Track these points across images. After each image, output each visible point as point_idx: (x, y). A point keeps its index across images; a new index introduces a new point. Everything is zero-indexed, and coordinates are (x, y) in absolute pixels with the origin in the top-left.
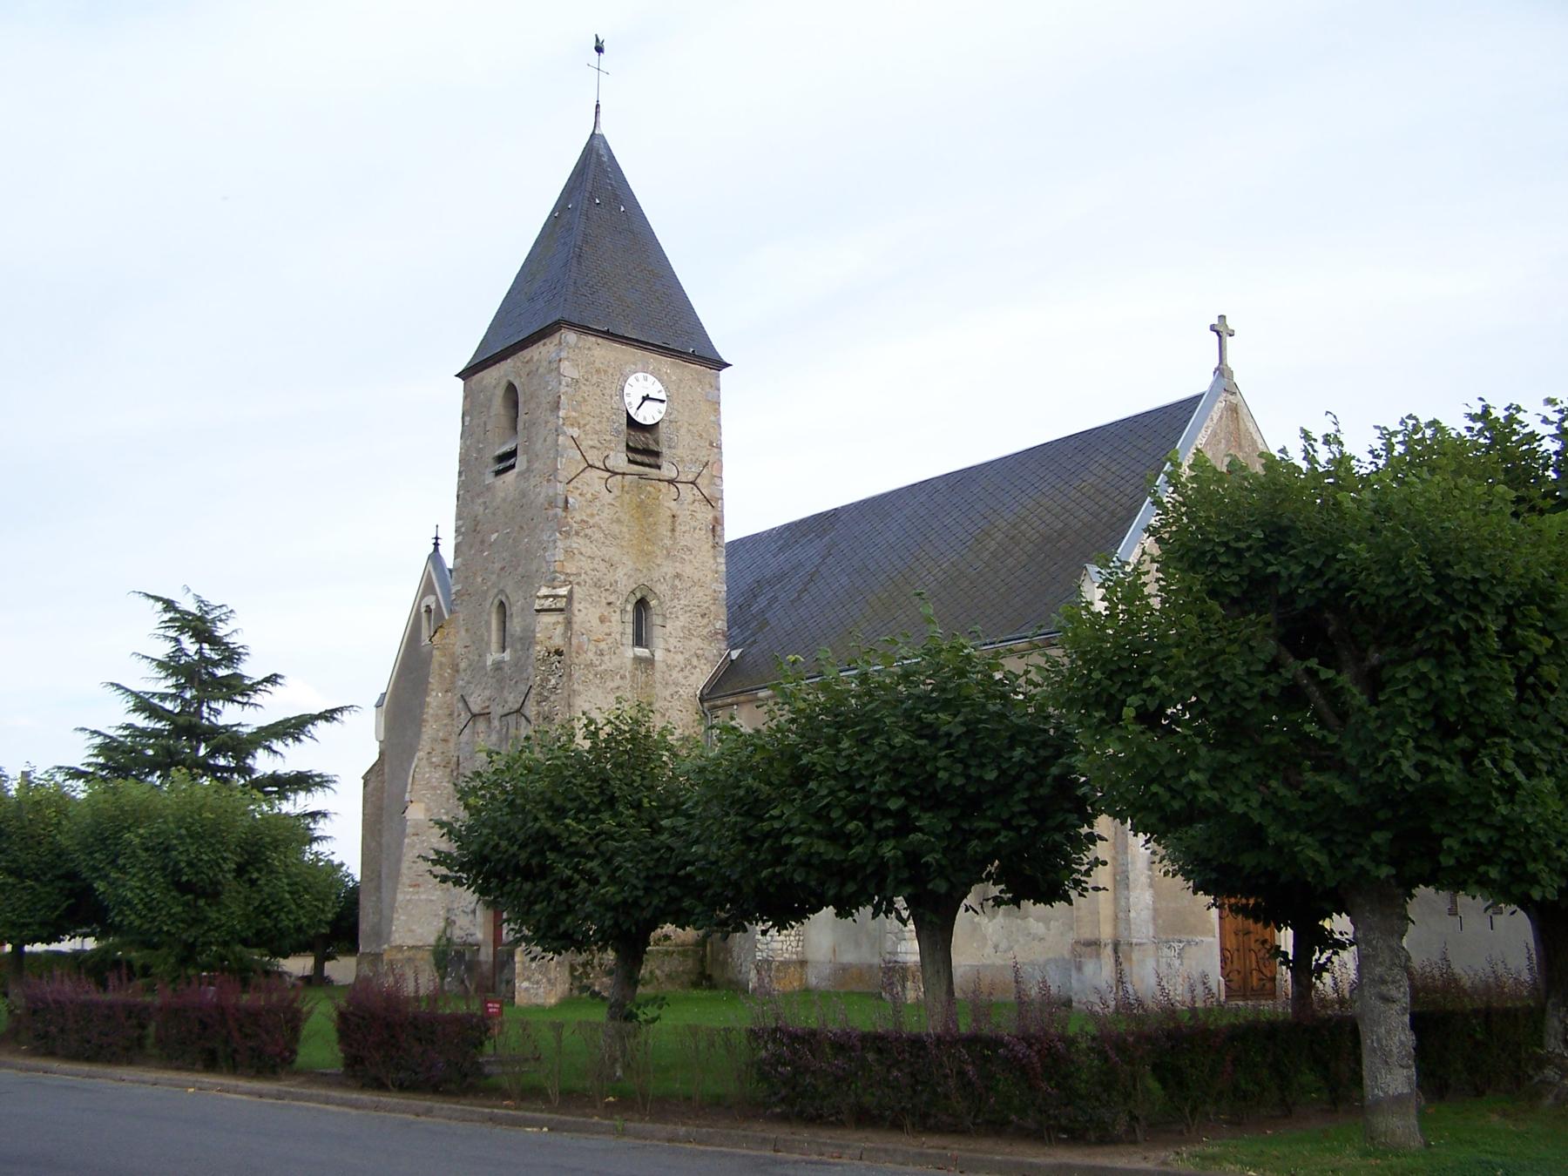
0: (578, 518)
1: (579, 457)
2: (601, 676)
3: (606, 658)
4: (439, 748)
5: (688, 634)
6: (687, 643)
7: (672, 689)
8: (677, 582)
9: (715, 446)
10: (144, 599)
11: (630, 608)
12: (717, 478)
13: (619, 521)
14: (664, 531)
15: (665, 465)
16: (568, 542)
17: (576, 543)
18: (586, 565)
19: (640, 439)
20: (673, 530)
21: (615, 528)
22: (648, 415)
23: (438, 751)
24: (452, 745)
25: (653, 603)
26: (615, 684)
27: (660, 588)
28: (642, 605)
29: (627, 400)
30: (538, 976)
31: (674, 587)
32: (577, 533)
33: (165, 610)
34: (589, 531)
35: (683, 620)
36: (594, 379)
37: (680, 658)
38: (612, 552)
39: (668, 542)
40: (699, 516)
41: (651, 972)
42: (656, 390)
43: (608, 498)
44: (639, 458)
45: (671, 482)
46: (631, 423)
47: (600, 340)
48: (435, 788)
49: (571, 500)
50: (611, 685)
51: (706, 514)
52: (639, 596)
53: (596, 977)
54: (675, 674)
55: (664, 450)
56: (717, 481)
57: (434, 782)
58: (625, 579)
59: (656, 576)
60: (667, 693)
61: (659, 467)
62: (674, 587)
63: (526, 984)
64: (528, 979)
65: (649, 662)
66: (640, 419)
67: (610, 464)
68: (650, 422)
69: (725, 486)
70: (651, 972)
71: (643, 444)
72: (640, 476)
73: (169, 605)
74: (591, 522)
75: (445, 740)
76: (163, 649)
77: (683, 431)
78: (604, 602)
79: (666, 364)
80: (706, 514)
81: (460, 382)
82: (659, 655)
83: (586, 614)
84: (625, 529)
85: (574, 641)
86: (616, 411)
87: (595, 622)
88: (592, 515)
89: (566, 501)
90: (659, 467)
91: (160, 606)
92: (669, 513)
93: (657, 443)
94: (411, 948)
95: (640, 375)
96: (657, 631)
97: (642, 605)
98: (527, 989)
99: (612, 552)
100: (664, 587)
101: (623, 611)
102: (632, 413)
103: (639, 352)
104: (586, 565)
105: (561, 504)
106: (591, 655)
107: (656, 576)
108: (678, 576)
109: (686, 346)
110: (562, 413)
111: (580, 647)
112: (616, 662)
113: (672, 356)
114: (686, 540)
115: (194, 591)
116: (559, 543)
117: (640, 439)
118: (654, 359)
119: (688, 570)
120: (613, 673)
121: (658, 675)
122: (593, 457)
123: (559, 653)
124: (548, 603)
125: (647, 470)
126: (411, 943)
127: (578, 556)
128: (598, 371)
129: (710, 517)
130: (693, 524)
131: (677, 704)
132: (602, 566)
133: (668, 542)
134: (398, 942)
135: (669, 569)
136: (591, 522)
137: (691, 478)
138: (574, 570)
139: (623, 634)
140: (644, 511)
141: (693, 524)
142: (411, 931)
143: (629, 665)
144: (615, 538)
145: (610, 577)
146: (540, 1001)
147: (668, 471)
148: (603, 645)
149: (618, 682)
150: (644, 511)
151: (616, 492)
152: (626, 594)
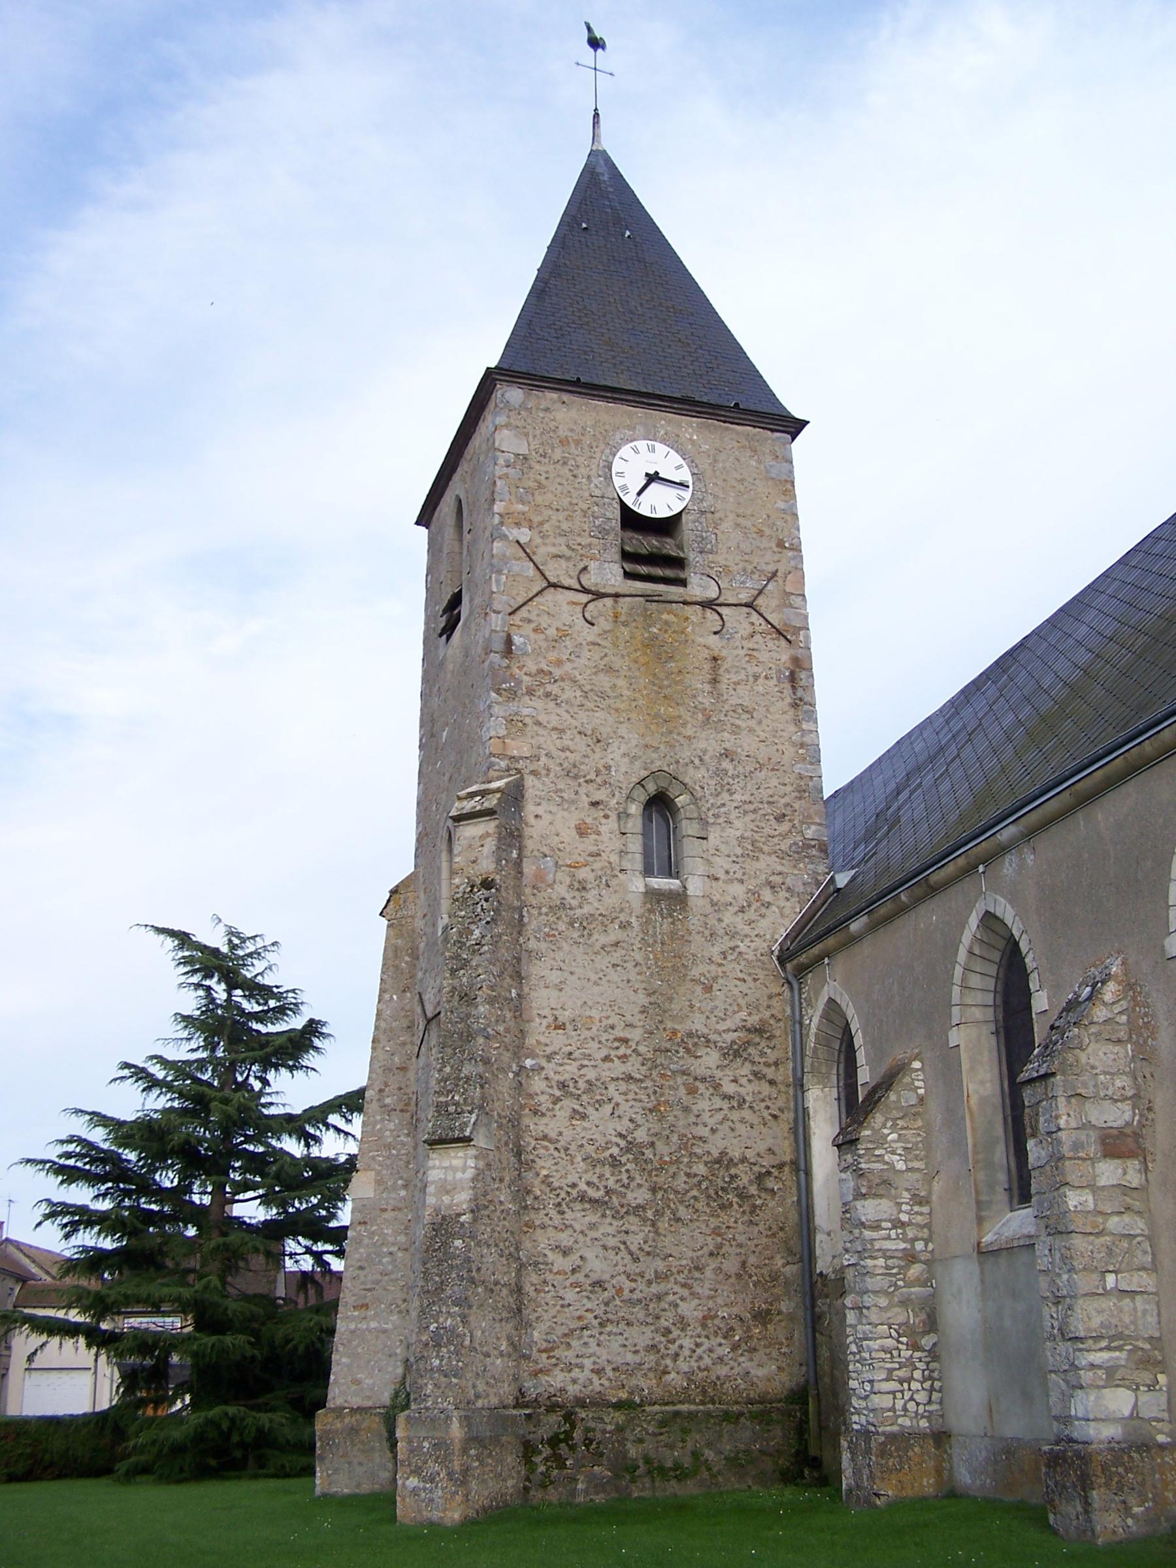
0: (532, 667)
1: (531, 571)
2: (585, 925)
3: (591, 895)
4: (394, 1081)
5: (753, 850)
6: (751, 866)
7: (725, 943)
8: (726, 764)
9: (790, 547)
10: (152, 933)
11: (635, 809)
12: (794, 596)
13: (610, 670)
14: (698, 682)
15: (694, 580)
16: (513, 706)
17: (527, 707)
18: (550, 742)
19: (648, 544)
20: (715, 681)
21: (604, 681)
22: (658, 504)
23: (394, 1086)
24: (411, 1074)
25: (681, 801)
26: (612, 937)
27: (692, 776)
28: (660, 805)
29: (618, 482)
30: (433, 1467)
31: (720, 773)
32: (530, 692)
33: (181, 947)
34: (554, 689)
35: (741, 826)
36: (558, 454)
37: (738, 890)
38: (601, 720)
39: (707, 701)
40: (763, 656)
41: (696, 1455)
42: (670, 464)
43: (590, 634)
44: (643, 570)
45: (708, 604)
46: (631, 520)
47: (565, 397)
48: (389, 1147)
49: (517, 640)
50: (600, 939)
51: (779, 655)
52: (652, 788)
53: (579, 1466)
54: (728, 917)
55: (692, 556)
56: (797, 601)
57: (388, 1137)
58: (625, 762)
59: (685, 754)
60: (715, 951)
61: (683, 583)
62: (720, 773)
63: (413, 1482)
64: (417, 1472)
65: (679, 899)
66: (644, 511)
67: (589, 581)
68: (663, 513)
69: (811, 609)
70: (696, 1455)
71: (653, 549)
72: (648, 598)
73: (183, 939)
74: (557, 672)
75: (403, 1069)
76: (191, 1003)
77: (726, 526)
78: (585, 800)
79: (690, 427)
80: (779, 655)
81: (423, 531)
82: (695, 886)
83: (549, 822)
84: (621, 682)
85: (529, 868)
86: (598, 500)
87: (569, 835)
88: (559, 663)
89: (509, 641)
90: (683, 583)
91: (171, 943)
92: (706, 654)
93: (682, 549)
94: (354, 1411)
95: (642, 445)
96: (690, 847)
97: (660, 805)
98: (415, 1492)
99: (601, 720)
100: (702, 772)
101: (623, 815)
102: (629, 501)
103: (640, 412)
104: (550, 742)
105: (498, 645)
106: (561, 890)
107: (685, 754)
108: (727, 754)
109: (729, 398)
110: (498, 507)
111: (540, 876)
112: (611, 900)
113: (699, 414)
114: (743, 696)
115: (225, 921)
116: (496, 709)
117: (648, 544)
118: (664, 420)
119: (747, 744)
120: (606, 920)
121: (694, 922)
122: (555, 571)
123: (487, 884)
124: (468, 806)
125: (661, 587)
126: (356, 1402)
127: (532, 728)
128: (564, 442)
129: (785, 657)
130: (752, 669)
131: (733, 968)
132: (581, 744)
133: (707, 701)
134: (339, 1402)
135: (709, 743)
136: (557, 672)
137: (744, 597)
138: (526, 751)
139: (622, 853)
140: (659, 653)
141: (752, 669)
142: (357, 1382)
143: (637, 903)
144: (603, 695)
145: (597, 758)
146: (436, 1515)
147: (699, 587)
148: (583, 873)
149: (615, 934)
150: (659, 653)
151: (604, 624)
152: (626, 786)
